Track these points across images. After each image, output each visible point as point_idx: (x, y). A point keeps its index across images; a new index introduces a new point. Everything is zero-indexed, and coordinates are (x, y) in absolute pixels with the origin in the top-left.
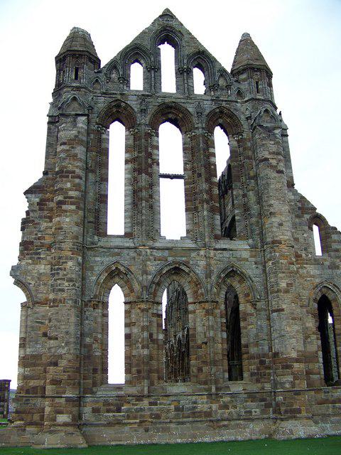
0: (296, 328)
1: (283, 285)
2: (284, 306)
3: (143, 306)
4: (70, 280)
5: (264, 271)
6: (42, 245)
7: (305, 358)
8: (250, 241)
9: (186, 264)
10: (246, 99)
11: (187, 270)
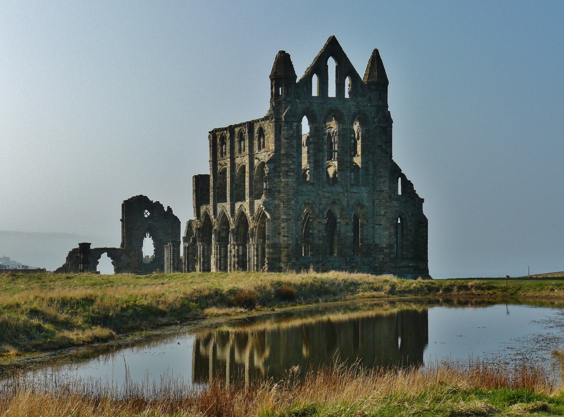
0: (386, 233)
1: (383, 212)
2: (382, 223)
3: (319, 220)
4: (293, 210)
5: (374, 204)
6: (276, 191)
7: (390, 246)
8: (368, 188)
9: (338, 200)
10: (373, 104)
11: (339, 203)
